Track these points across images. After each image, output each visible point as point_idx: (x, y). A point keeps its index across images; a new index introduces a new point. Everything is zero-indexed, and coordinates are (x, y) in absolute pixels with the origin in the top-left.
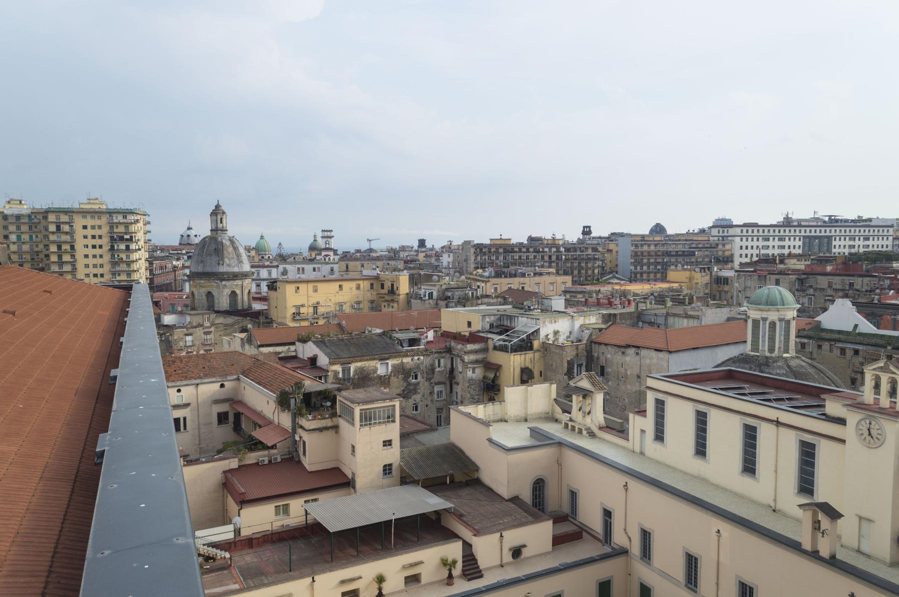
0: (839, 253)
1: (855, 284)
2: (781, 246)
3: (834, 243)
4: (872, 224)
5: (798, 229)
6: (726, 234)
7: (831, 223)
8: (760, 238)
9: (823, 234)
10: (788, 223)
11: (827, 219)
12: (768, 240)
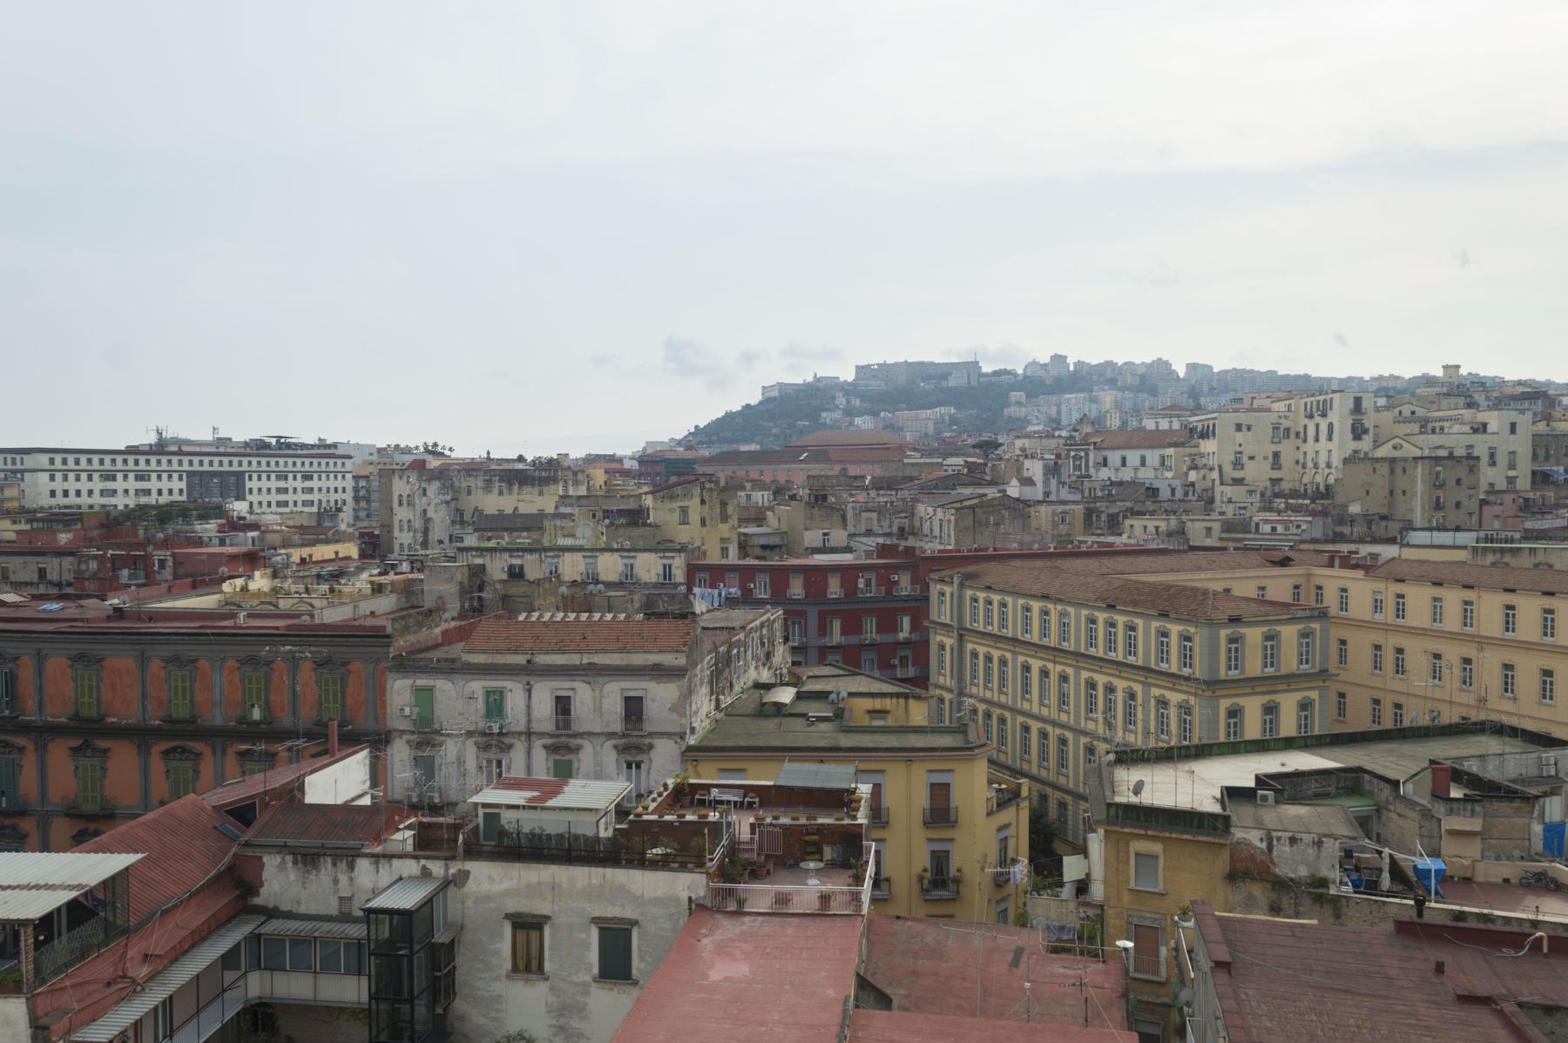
0: (91, 507)
1: (48, 571)
2: (143, 490)
3: (248, 485)
4: (338, 452)
5: (175, 459)
6: (19, 466)
7: (280, 449)
8: (96, 476)
9: (226, 468)
10: (160, 448)
11: (274, 441)
12: (114, 479)
